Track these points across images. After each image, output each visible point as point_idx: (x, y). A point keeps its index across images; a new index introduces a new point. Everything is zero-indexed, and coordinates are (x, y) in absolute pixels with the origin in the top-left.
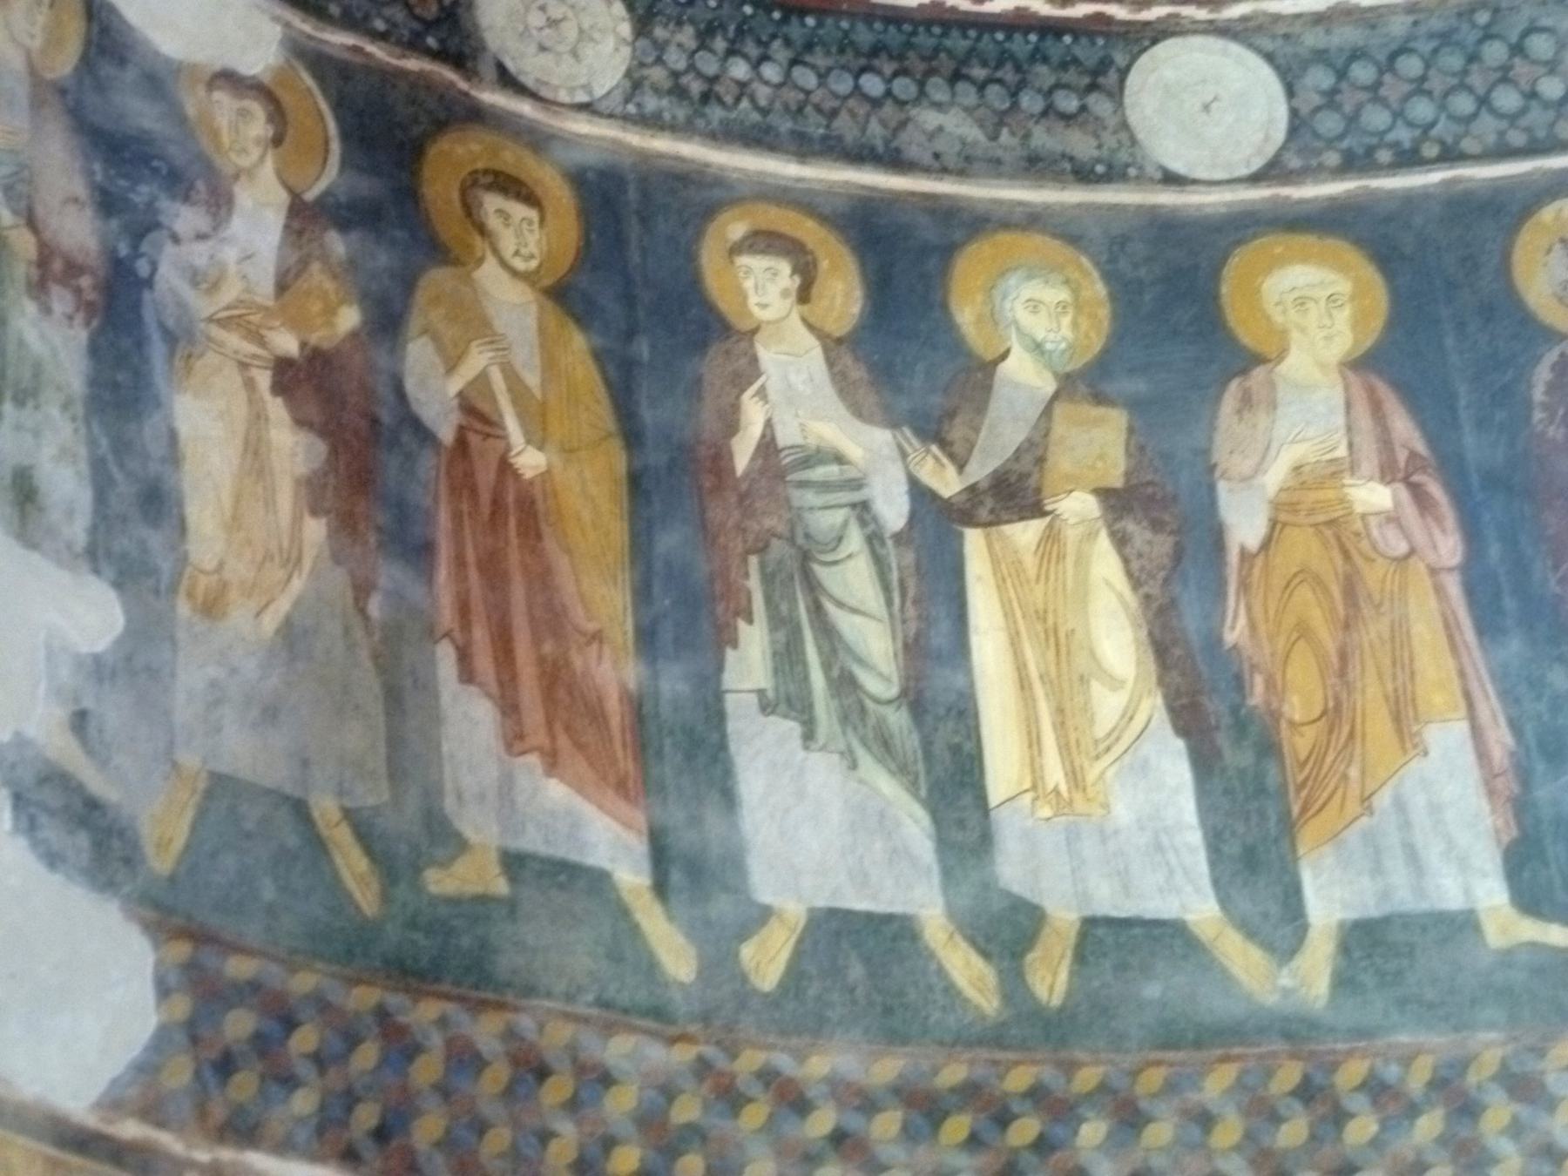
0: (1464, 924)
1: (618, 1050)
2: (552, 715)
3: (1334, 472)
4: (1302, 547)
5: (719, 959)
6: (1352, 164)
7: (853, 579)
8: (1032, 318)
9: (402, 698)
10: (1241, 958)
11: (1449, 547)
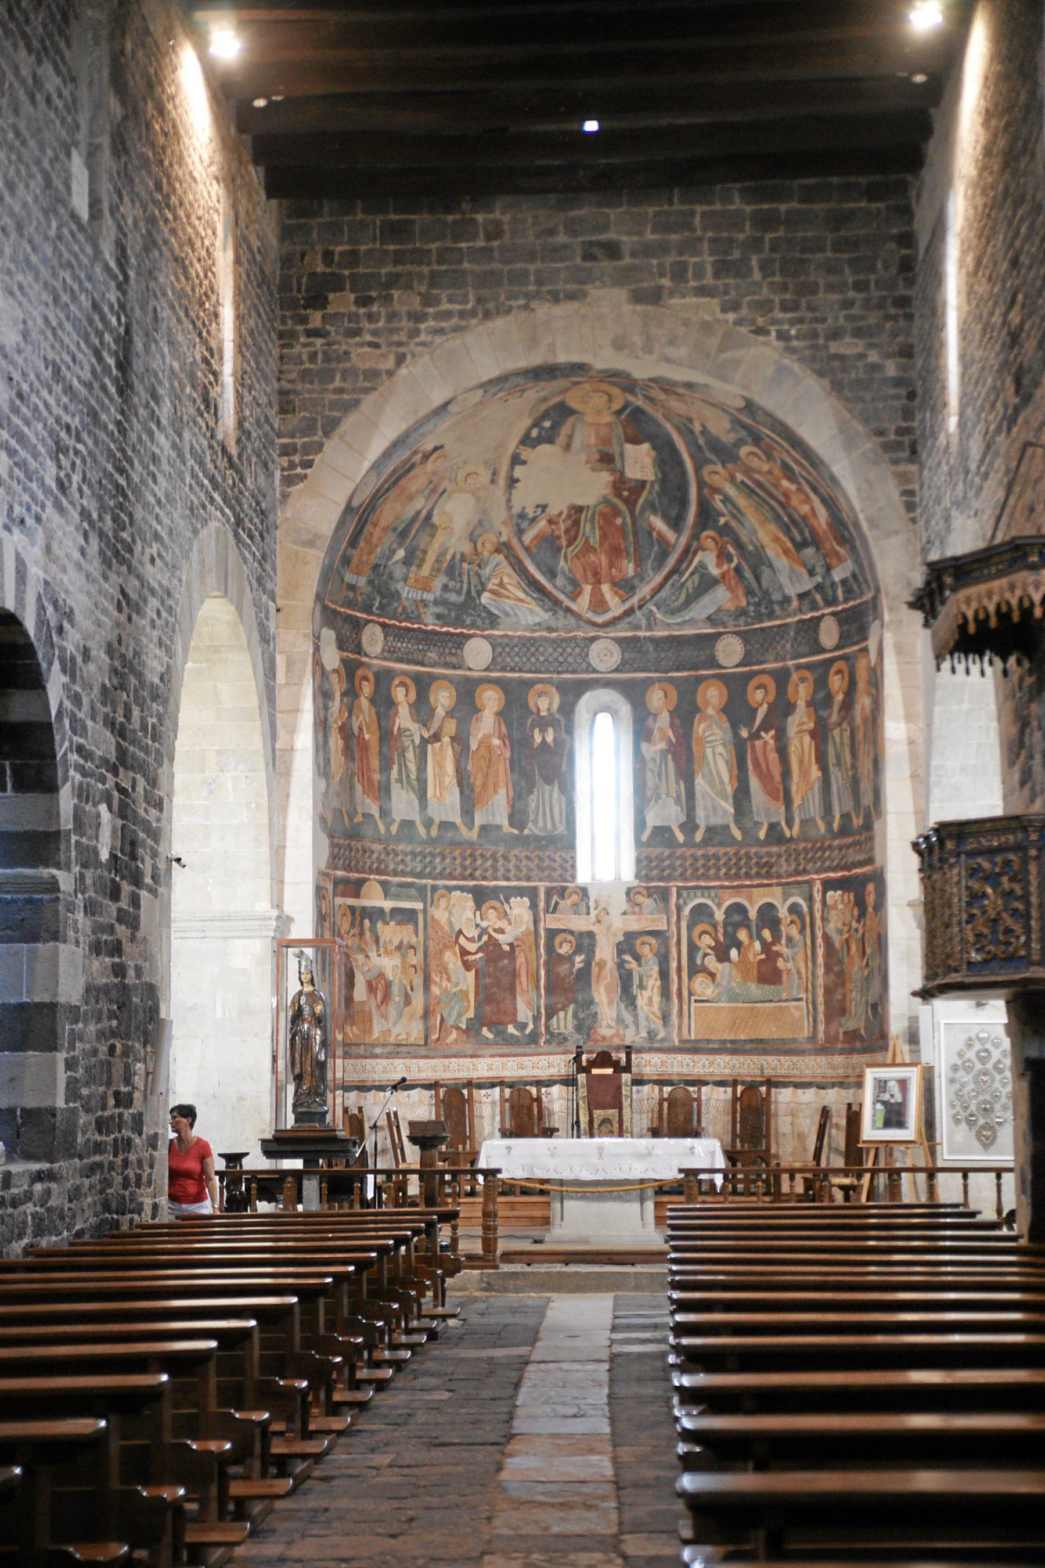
0: (499, 827)
1: (377, 847)
2: (369, 787)
3: (490, 736)
4: (483, 751)
5: (388, 830)
6: (503, 669)
7: (410, 755)
8: (443, 698)
9: (352, 788)
10: (463, 829)
11: (508, 755)
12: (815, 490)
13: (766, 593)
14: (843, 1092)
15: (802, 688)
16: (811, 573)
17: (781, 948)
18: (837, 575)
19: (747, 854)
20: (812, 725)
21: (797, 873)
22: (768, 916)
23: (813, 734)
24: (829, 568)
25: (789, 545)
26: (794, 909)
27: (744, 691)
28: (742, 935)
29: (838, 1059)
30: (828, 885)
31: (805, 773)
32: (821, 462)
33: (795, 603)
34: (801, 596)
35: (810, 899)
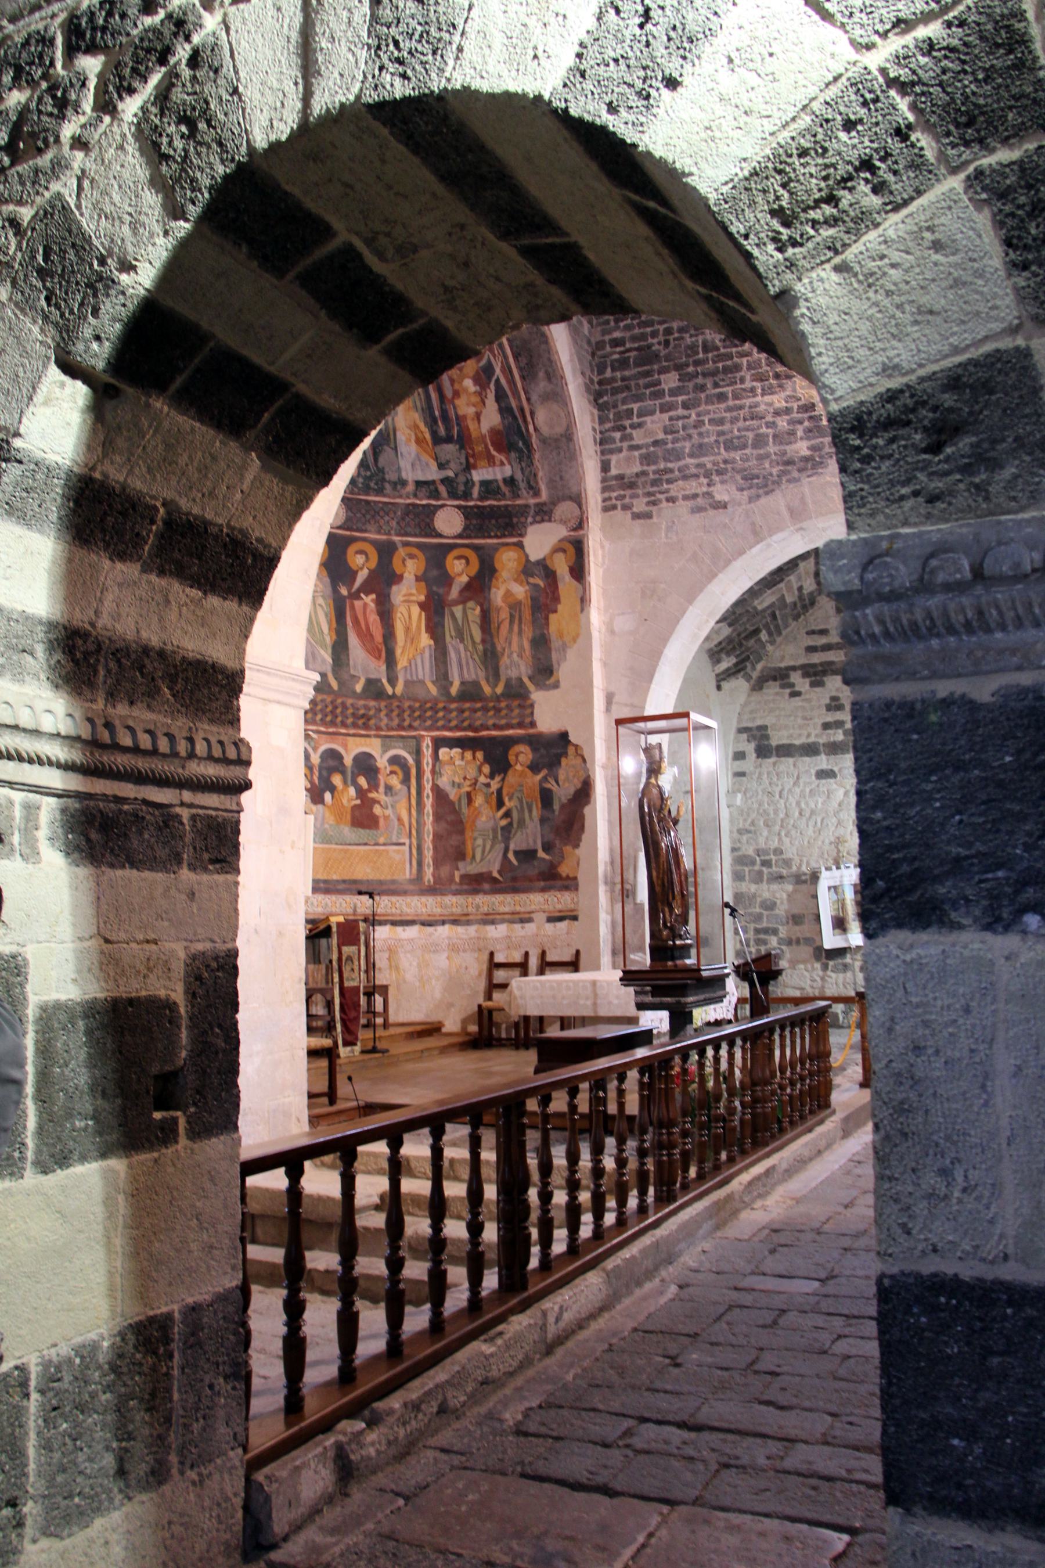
12: (501, 396)
13: (381, 471)
14: (460, 930)
15: (411, 564)
16: (441, 466)
17: (379, 795)
18: (477, 476)
19: (344, 705)
20: (422, 598)
21: (401, 727)
22: (365, 765)
23: (422, 606)
24: (468, 467)
25: (428, 436)
26: (395, 760)
27: (344, 553)
28: (337, 780)
29: (450, 900)
30: (438, 743)
31: (411, 639)
32: (554, 374)
33: (411, 488)
34: (419, 484)
35: (418, 753)
